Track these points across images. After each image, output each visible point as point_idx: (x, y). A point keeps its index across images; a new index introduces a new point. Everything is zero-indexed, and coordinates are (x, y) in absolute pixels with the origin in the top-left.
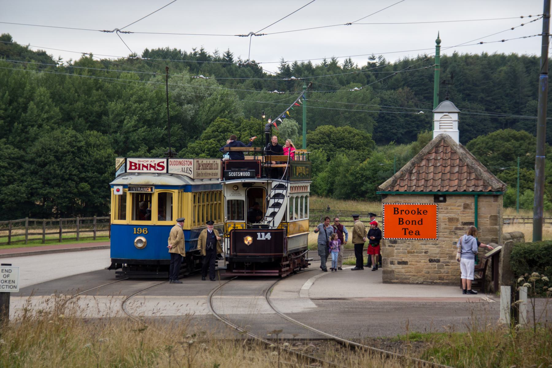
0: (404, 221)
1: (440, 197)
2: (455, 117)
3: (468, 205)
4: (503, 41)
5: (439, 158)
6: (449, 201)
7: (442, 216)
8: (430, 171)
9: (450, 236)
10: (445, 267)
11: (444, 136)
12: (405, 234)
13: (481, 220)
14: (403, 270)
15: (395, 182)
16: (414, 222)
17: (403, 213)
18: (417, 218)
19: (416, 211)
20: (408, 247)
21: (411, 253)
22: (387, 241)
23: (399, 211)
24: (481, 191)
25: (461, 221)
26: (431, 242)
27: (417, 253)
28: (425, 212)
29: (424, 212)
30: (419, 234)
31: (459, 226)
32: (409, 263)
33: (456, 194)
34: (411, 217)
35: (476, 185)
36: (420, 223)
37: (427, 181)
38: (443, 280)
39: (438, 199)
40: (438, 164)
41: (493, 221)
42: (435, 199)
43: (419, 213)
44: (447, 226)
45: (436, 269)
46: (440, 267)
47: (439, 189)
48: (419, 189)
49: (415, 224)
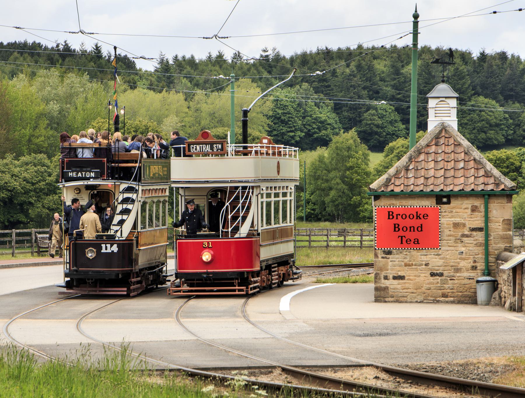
0: (401, 227)
1: (443, 198)
2: (454, 103)
3: (476, 207)
4: (520, 10)
5: (440, 151)
6: (454, 203)
8: (430, 167)
9: (455, 245)
10: (450, 282)
11: (446, 125)
12: (402, 243)
13: (491, 225)
14: (399, 287)
15: (388, 180)
16: (412, 229)
17: (399, 217)
18: (416, 223)
21: (409, 266)
22: (379, 251)
23: (394, 215)
24: (492, 190)
25: (468, 226)
26: (433, 252)
27: (415, 265)
28: (426, 216)
29: (424, 216)
30: (418, 243)
31: (466, 233)
32: (406, 278)
33: (462, 195)
34: (408, 223)
35: (486, 183)
36: (420, 229)
37: (427, 178)
38: (447, 297)
40: (440, 159)
41: (506, 226)
43: (418, 217)
44: (452, 233)
45: (439, 285)
46: (444, 282)
47: (442, 188)
48: (418, 189)
49: (414, 231)
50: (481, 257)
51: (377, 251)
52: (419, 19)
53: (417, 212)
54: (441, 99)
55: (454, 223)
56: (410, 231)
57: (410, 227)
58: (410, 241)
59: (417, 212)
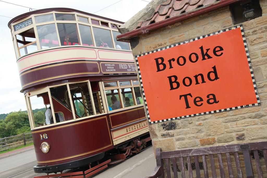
0: (180, 80)
12: (188, 107)
17: (174, 64)
18: (203, 67)
19: (199, 52)
20: (199, 131)
23: (166, 62)
28: (218, 51)
29: (215, 52)
30: (216, 102)
34: (191, 69)
36: (212, 76)
43: (205, 56)
49: (203, 81)
51: (153, 126)
53: (201, 48)
56: (197, 83)
57: (196, 77)
58: (201, 100)
59: (201, 48)
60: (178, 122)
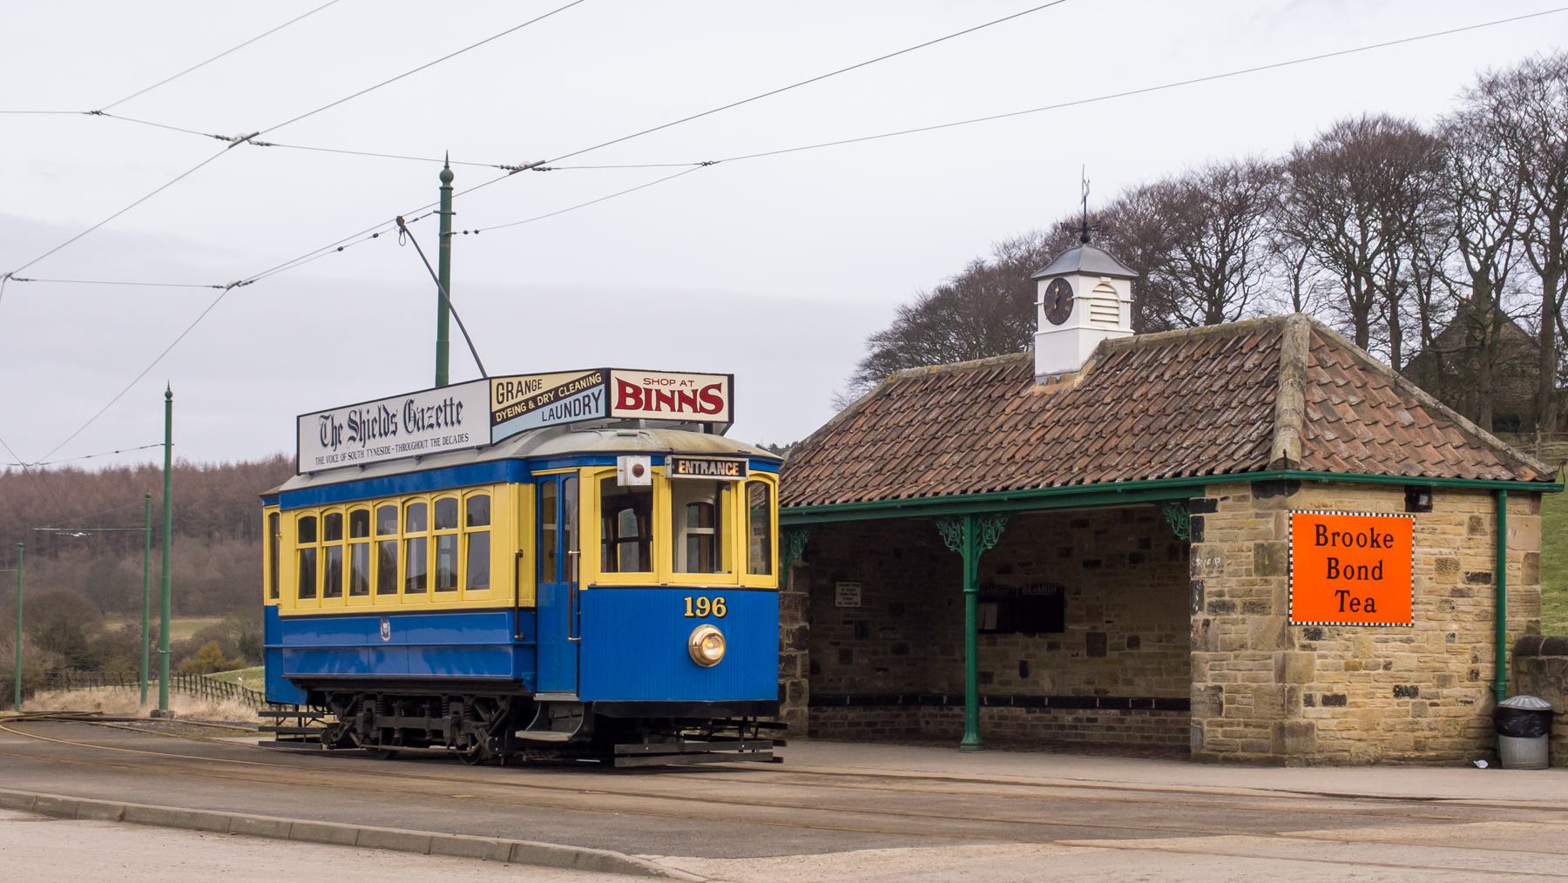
0: (1341, 568)
1: (1417, 495)
2: (1124, 290)
6: (1443, 506)
7: (1423, 554)
16: (1362, 572)
18: (1369, 556)
20: (1348, 648)
21: (1355, 668)
25: (1464, 568)
27: (1366, 668)
28: (1388, 539)
31: (1461, 586)
32: (1349, 700)
39: (1417, 499)
42: (1408, 500)
50: (1486, 647)
52: (452, 184)
54: (1104, 279)
55: (1438, 561)
60: (1326, 629)
